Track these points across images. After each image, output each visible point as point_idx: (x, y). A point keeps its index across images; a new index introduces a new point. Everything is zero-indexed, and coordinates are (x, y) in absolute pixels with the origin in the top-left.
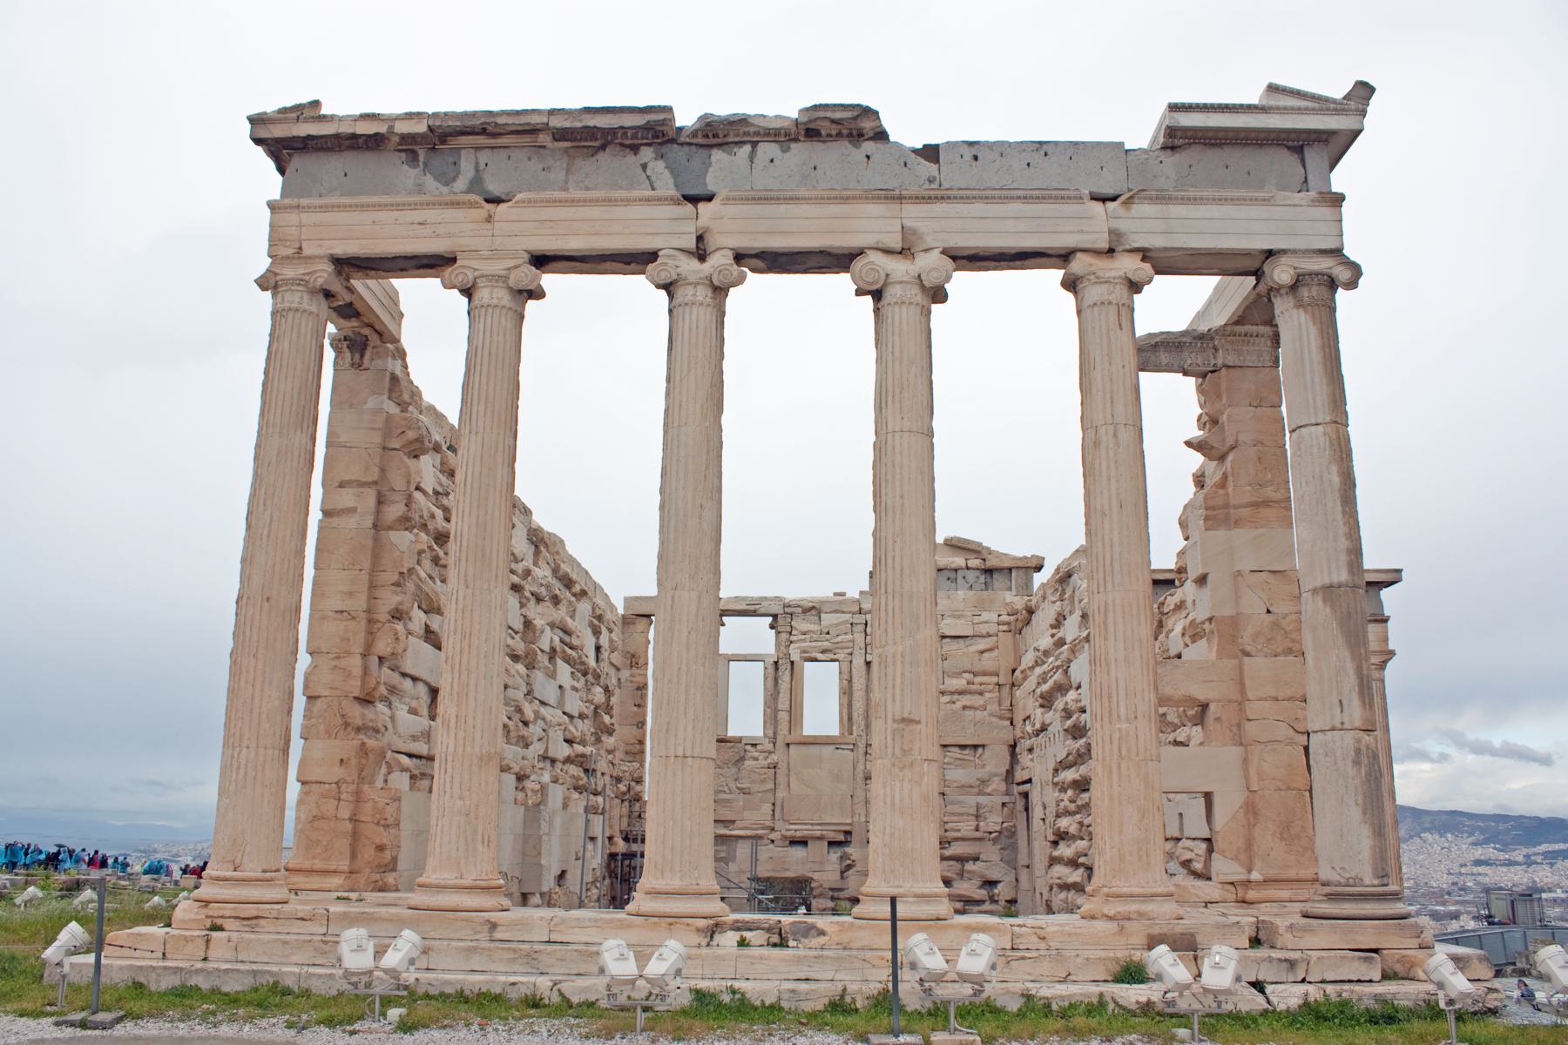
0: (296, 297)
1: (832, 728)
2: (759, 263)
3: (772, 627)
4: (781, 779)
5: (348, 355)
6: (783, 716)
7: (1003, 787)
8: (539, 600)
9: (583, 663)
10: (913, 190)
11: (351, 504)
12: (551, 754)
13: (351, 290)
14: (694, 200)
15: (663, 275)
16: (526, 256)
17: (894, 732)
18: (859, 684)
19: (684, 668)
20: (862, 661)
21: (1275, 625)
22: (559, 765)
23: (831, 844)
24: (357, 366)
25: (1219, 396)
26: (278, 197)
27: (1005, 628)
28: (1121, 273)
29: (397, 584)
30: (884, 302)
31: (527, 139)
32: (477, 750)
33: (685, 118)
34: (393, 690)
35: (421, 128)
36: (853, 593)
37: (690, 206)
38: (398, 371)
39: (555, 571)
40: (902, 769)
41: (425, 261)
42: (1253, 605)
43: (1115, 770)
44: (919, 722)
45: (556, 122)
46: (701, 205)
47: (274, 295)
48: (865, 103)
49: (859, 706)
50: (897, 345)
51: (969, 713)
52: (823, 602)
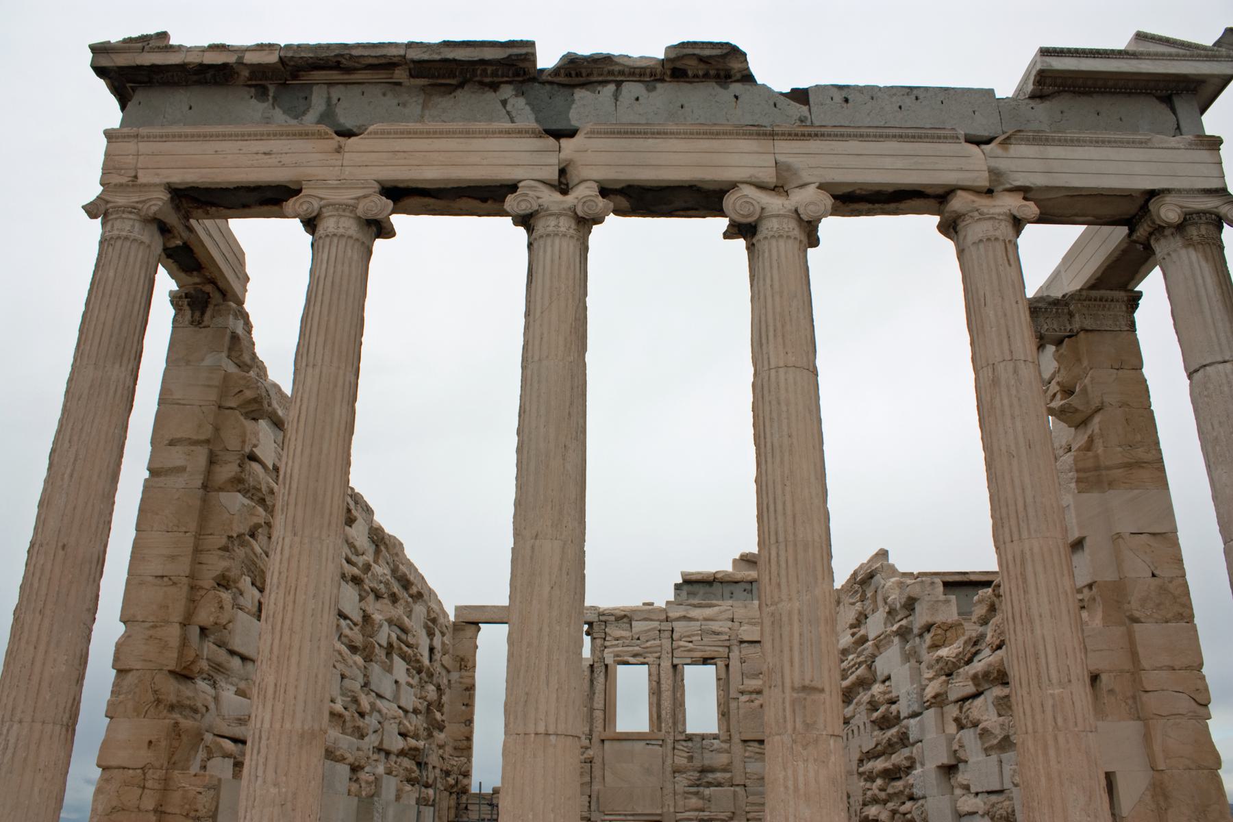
0: (127, 225)
2: (624, 203)
4: (597, 772)
5: (188, 313)
6: (599, 714)
8: (378, 596)
9: (418, 661)
10: (786, 128)
11: (179, 462)
12: (385, 746)
13: (190, 229)
14: (558, 135)
15: (523, 205)
16: (377, 187)
17: (793, 702)
18: (666, 684)
19: (546, 629)
20: (669, 664)
21: (1163, 590)
22: (393, 758)
24: (197, 323)
25: (1079, 360)
26: (117, 126)
28: (1005, 210)
29: (225, 549)
30: (759, 236)
31: (381, 75)
32: (298, 725)
33: (546, 60)
34: (218, 668)
35: (273, 58)
36: (660, 603)
37: (551, 141)
38: (240, 331)
39: (394, 571)
40: (805, 747)
41: (269, 195)
42: (1137, 568)
43: (1051, 742)
44: (822, 691)
45: (413, 55)
46: (564, 142)
47: (104, 224)
48: (733, 43)
49: (667, 704)
50: (776, 277)
52: (634, 611)
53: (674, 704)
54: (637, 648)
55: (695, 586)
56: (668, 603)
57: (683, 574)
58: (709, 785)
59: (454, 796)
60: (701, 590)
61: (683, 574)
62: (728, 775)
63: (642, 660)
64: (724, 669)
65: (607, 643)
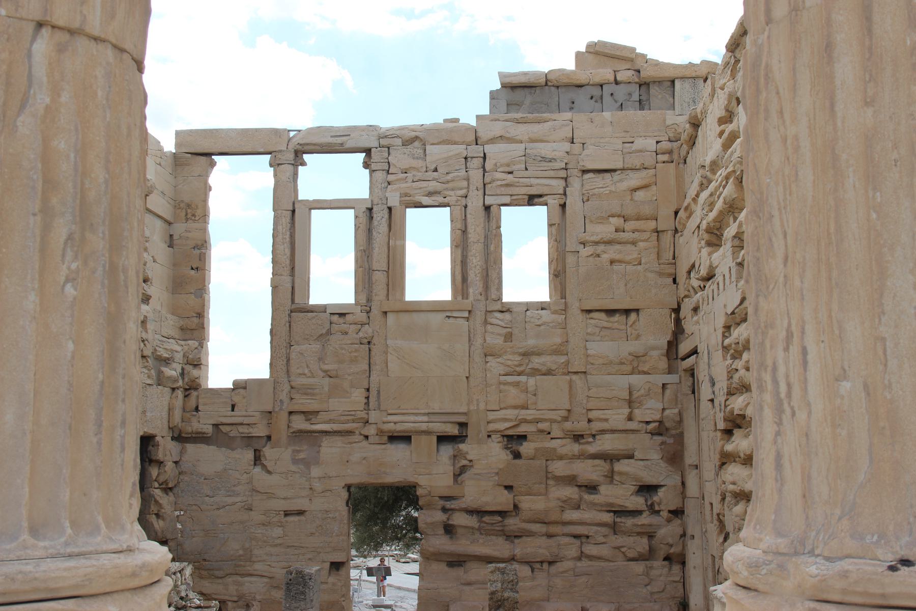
1: (443, 292)
4: (377, 358)
6: (379, 278)
7: (663, 364)
23: (443, 439)
27: (666, 157)
49: (476, 261)
51: (616, 267)
53: (486, 262)
54: (434, 183)
55: (522, 93)
56: (479, 117)
57: (502, 75)
58: (535, 372)
59: (180, 394)
60: (528, 98)
61: (502, 75)
62: (563, 359)
63: (440, 199)
64: (558, 210)
65: (391, 178)
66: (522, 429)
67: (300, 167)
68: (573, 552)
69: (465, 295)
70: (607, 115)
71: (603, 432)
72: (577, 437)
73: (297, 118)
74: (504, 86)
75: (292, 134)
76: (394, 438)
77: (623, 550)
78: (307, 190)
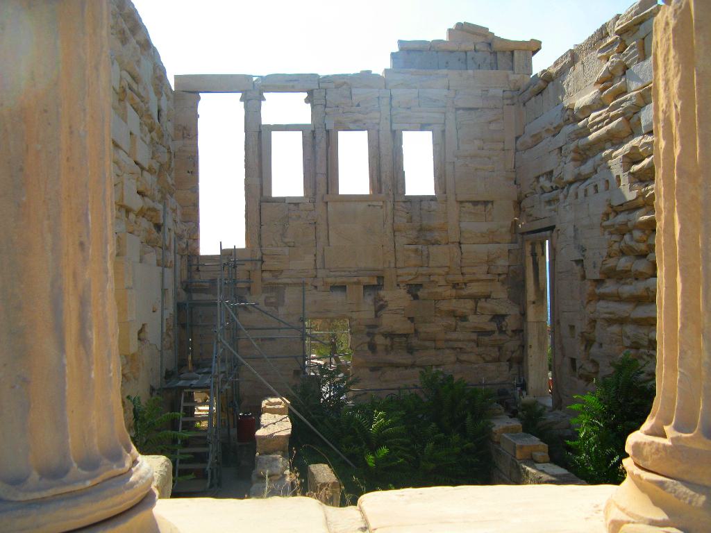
3: (307, 101)
9: (150, 116)
12: (126, 203)
22: (132, 216)
27: (509, 102)
55: (413, 56)
57: (400, 42)
61: (400, 42)
66: (419, 281)
67: (262, 102)
68: (453, 358)
69: (380, 192)
70: (470, 72)
71: (471, 281)
72: (455, 285)
73: (258, 69)
74: (401, 49)
75: (254, 79)
76: (334, 288)
77: (483, 356)
78: (267, 118)
